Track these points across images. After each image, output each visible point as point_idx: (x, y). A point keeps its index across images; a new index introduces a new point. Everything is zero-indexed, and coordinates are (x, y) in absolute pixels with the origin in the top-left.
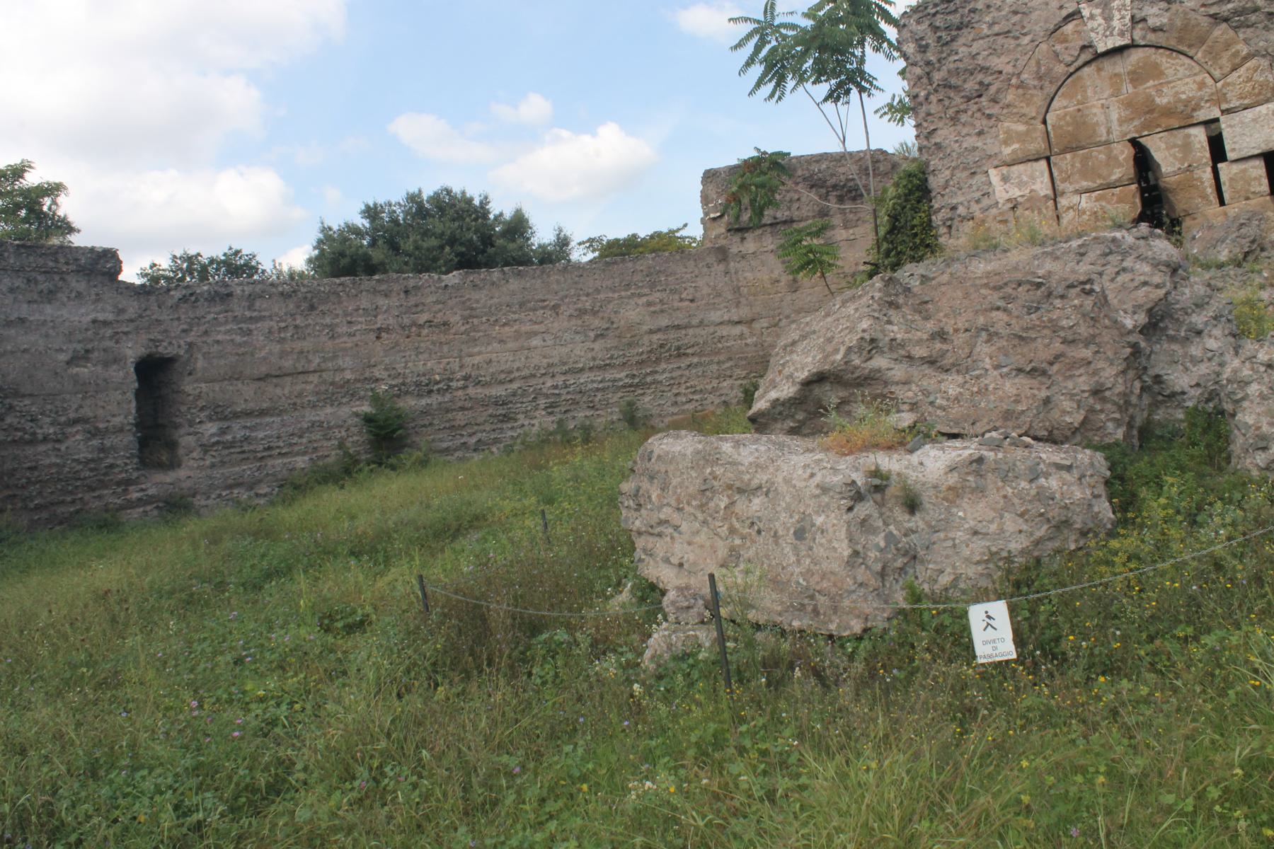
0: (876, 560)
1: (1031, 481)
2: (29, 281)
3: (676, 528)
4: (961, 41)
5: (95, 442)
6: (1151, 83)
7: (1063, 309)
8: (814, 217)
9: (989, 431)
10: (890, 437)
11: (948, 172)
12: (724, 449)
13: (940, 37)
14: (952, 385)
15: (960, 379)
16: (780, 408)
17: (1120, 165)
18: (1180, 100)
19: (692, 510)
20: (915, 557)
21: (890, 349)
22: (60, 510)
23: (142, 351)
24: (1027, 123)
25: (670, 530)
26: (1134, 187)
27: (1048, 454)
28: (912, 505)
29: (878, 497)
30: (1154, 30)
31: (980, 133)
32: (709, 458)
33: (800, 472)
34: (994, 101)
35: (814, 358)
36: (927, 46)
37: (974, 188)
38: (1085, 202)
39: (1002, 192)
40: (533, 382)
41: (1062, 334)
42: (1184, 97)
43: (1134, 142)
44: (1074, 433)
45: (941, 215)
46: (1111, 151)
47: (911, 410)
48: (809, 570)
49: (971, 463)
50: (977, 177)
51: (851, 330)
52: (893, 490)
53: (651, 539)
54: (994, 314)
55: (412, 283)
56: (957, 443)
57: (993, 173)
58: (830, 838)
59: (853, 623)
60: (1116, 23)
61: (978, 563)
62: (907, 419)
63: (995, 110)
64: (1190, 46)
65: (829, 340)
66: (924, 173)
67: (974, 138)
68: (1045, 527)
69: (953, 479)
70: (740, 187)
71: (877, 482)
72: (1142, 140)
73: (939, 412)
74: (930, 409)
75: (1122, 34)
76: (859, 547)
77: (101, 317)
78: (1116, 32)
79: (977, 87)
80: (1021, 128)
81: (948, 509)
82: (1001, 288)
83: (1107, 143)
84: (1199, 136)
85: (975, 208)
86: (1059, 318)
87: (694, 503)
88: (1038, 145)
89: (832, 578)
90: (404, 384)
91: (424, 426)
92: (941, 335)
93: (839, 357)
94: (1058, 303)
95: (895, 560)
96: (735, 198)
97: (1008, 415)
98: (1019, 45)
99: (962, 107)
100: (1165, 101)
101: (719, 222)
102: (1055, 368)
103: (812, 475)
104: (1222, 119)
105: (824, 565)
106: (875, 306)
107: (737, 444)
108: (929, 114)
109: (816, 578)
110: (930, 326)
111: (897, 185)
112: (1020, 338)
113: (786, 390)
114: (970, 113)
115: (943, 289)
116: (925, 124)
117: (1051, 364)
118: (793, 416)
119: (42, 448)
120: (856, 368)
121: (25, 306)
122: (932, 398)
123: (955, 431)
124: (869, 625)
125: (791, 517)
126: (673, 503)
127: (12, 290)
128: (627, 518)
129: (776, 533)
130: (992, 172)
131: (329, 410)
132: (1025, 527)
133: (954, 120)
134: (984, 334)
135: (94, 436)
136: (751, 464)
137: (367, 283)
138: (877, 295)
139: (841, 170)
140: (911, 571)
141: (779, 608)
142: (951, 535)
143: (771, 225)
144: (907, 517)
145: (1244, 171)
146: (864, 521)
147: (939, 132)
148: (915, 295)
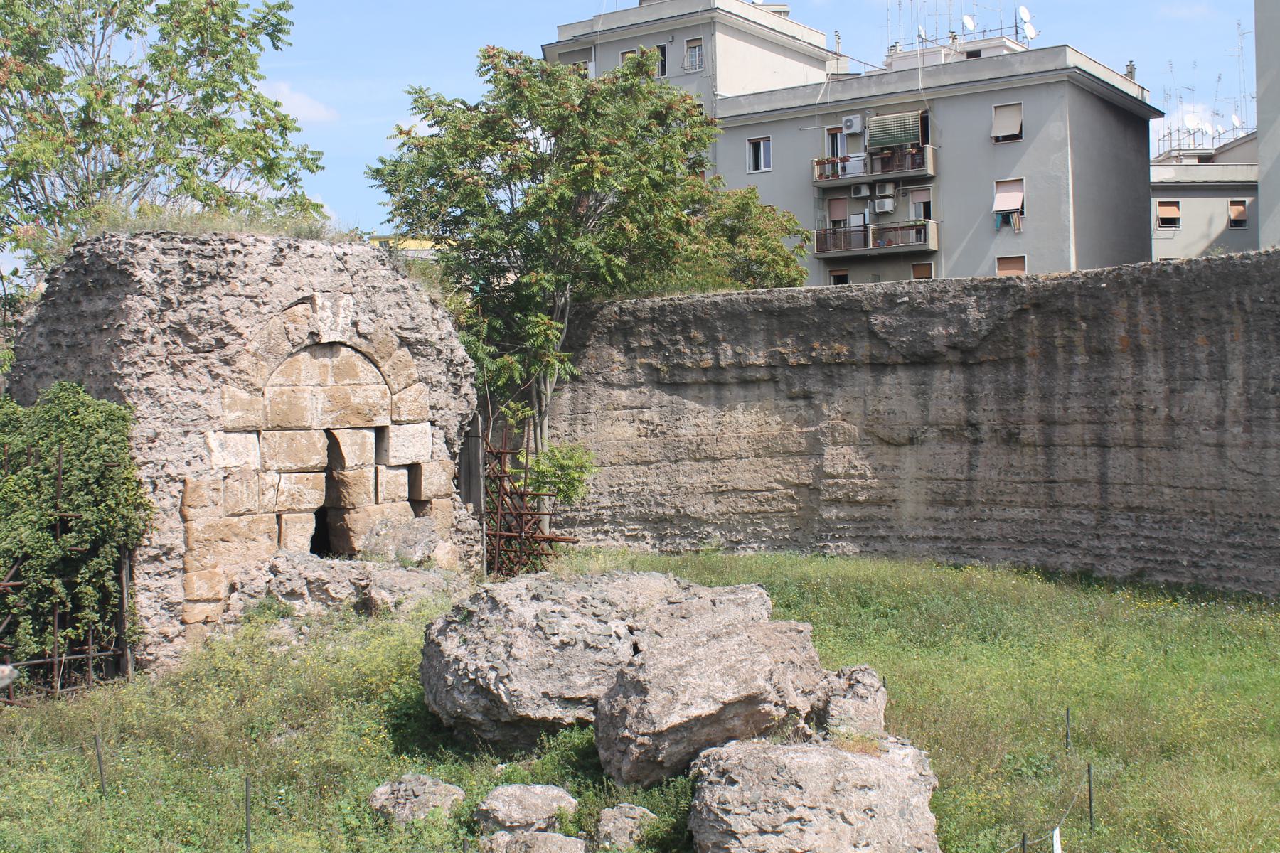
4: (210, 290)
6: (348, 381)
13: (190, 280)
18: (367, 404)
24: (250, 392)
26: (324, 475)
31: (204, 392)
34: (227, 362)
36: (172, 282)
37: (186, 448)
38: (286, 482)
39: (220, 459)
46: (311, 437)
57: (214, 439)
60: (340, 320)
64: (382, 358)
75: (343, 332)
79: (213, 342)
80: (245, 395)
83: (308, 429)
84: (371, 435)
88: (255, 419)
100: (357, 401)
104: (392, 428)
108: (150, 355)
114: (196, 366)
116: (141, 364)
133: (176, 368)
147: (153, 376)
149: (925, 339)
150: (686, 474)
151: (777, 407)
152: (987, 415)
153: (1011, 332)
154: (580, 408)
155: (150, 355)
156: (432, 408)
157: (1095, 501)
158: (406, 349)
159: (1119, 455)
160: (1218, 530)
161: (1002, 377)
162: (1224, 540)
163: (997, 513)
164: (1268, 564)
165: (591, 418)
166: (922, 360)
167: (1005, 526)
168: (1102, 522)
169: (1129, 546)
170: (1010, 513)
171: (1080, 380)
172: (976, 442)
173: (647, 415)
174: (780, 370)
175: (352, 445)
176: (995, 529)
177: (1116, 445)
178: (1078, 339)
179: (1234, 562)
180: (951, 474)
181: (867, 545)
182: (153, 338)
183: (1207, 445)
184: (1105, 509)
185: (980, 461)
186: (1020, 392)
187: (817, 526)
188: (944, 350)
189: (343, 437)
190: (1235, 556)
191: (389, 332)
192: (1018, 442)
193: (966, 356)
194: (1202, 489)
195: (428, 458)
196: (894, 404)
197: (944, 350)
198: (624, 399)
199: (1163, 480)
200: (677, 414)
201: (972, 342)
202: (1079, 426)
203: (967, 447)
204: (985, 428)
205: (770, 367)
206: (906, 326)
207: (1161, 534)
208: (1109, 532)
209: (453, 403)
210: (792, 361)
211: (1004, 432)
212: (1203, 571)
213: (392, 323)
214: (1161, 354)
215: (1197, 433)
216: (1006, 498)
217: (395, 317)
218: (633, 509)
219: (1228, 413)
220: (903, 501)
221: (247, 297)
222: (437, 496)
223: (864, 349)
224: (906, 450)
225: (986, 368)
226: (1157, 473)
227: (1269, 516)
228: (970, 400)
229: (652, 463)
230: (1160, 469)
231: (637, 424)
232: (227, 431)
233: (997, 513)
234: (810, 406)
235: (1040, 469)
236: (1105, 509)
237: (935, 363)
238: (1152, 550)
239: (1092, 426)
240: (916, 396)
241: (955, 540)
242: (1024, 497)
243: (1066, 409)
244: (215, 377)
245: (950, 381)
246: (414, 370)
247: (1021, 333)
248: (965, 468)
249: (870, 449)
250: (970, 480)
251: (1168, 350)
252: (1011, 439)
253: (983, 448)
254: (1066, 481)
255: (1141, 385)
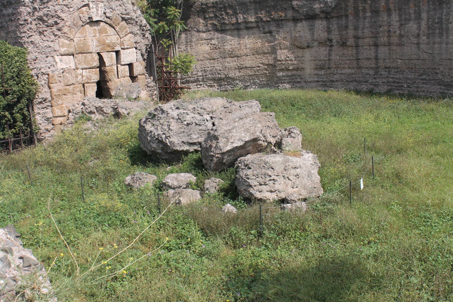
6: (104, 35)
17: (96, 62)
18: (112, 43)
24: (69, 41)
26: (98, 69)
30: (107, 17)
31: (52, 41)
34: (59, 30)
37: (48, 62)
38: (85, 72)
39: (60, 66)
42: (113, 42)
43: (98, 54)
46: (93, 56)
57: (57, 59)
60: (99, 12)
63: (59, 33)
64: (116, 25)
72: (101, 53)
75: (101, 17)
78: (99, 15)
79: (53, 23)
80: (67, 42)
83: (91, 53)
84: (114, 54)
88: (72, 50)
98: (69, 11)
99: (46, 29)
104: (122, 51)
108: (31, 29)
114: (48, 32)
116: (28, 32)
133: (41, 33)
145: (125, 68)
147: (33, 36)
149: (312, 9)
150: (228, 63)
151: (259, 37)
152: (335, 36)
153: (343, 5)
154: (189, 40)
155: (31, 29)
156: (136, 43)
157: (374, 66)
158: (124, 22)
159: (382, 49)
160: (417, 74)
161: (340, 22)
162: (419, 78)
163: (339, 71)
164: (435, 85)
165: (193, 44)
166: (311, 17)
167: (342, 76)
168: (376, 73)
169: (386, 81)
170: (344, 71)
171: (368, 22)
172: (331, 46)
173: (213, 42)
174: (260, 23)
175: (108, 58)
176: (338, 77)
177: (381, 45)
178: (367, 7)
179: (423, 85)
180: (322, 58)
181: (293, 85)
182: (31, 22)
183: (413, 44)
184: (377, 68)
185: (333, 53)
186: (347, 27)
187: (275, 79)
188: (319, 13)
189: (104, 55)
190: (423, 83)
191: (118, 15)
192: (346, 45)
193: (327, 15)
194: (412, 59)
195: (135, 61)
196: (302, 34)
197: (319, 13)
198: (204, 36)
199: (398, 57)
200: (224, 41)
201: (329, 10)
202: (368, 39)
203: (328, 48)
204: (334, 41)
205: (256, 22)
206: (305, 5)
207: (397, 76)
208: (379, 76)
209: (143, 41)
210: (264, 19)
211: (341, 42)
212: (412, 89)
213: (118, 12)
214: (397, 11)
215: (410, 40)
216: (342, 66)
217: (119, 10)
218: (210, 76)
219: (421, 32)
220: (306, 68)
221: (64, 5)
222: (139, 75)
223: (290, 14)
224: (306, 50)
225: (334, 19)
226: (396, 54)
227: (435, 68)
228: (329, 31)
229: (215, 59)
230: (397, 53)
231: (209, 45)
232: (62, 55)
233: (339, 71)
234: (272, 36)
235: (354, 55)
236: (377, 68)
237: (316, 18)
238: (394, 82)
239: (372, 39)
240: (309, 30)
241: (324, 82)
242: (349, 65)
243: (363, 33)
244: (56, 36)
245: (321, 24)
246: (128, 29)
247: (347, 6)
248: (328, 56)
249: (293, 50)
250: (329, 60)
251: (400, 10)
252: (344, 44)
253: (334, 48)
254: (364, 59)
255: (390, 23)
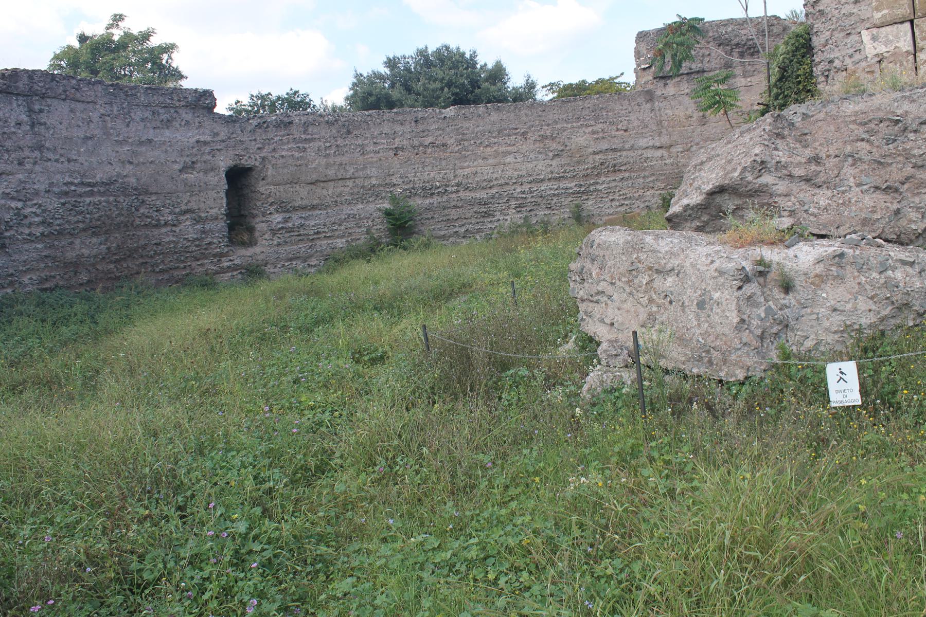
0: (758, 327)
1: (881, 273)
2: (154, 113)
3: (610, 297)
5: (199, 227)
7: (915, 141)
8: (720, 68)
9: (850, 234)
10: (773, 236)
11: (828, 33)
12: (647, 240)
14: (823, 198)
15: (829, 193)
16: (689, 212)
19: (621, 284)
20: (787, 326)
21: (776, 169)
22: (176, 273)
23: (231, 163)
25: (605, 299)
27: (896, 252)
28: (787, 288)
29: (761, 280)
32: (634, 247)
33: (703, 259)
35: (717, 174)
37: (849, 46)
39: (871, 49)
40: (507, 188)
41: (913, 160)
44: (917, 237)
45: (820, 67)
47: (790, 216)
48: (706, 332)
49: (834, 257)
50: (851, 37)
51: (746, 154)
52: (771, 276)
53: (591, 304)
54: (859, 144)
55: (420, 115)
56: (825, 242)
57: (866, 35)
58: (713, 525)
59: (737, 372)
61: (835, 332)
62: (786, 222)
65: (729, 162)
66: (809, 34)
67: (852, 6)
68: (890, 308)
69: (819, 269)
70: (665, 45)
71: (761, 268)
73: (811, 218)
74: (805, 215)
76: (745, 317)
77: (202, 138)
81: (814, 292)
82: (866, 124)
85: (848, 61)
86: (911, 148)
87: (623, 279)
89: (724, 338)
90: (413, 188)
91: (428, 219)
92: (816, 160)
93: (736, 174)
94: (912, 136)
95: (772, 328)
96: (661, 54)
97: (865, 222)
101: (647, 72)
102: (906, 186)
103: (712, 262)
105: (719, 328)
106: (766, 137)
107: (657, 237)
109: (712, 338)
110: (808, 152)
111: (787, 43)
112: (880, 163)
113: (695, 199)
115: (820, 124)
117: (903, 183)
118: (699, 218)
119: (164, 230)
120: (749, 183)
121: (151, 131)
122: (806, 207)
123: (823, 233)
124: (750, 374)
125: (695, 292)
126: (608, 279)
127: (142, 120)
128: (574, 289)
129: (683, 303)
130: (865, 33)
131: (360, 206)
132: (874, 307)
134: (850, 159)
135: (198, 222)
136: (666, 252)
137: (388, 114)
138: (768, 128)
139: (743, 32)
140: (784, 336)
141: (683, 359)
142: (816, 311)
143: (687, 74)
144: (783, 296)
146: (750, 297)
148: (797, 128)
